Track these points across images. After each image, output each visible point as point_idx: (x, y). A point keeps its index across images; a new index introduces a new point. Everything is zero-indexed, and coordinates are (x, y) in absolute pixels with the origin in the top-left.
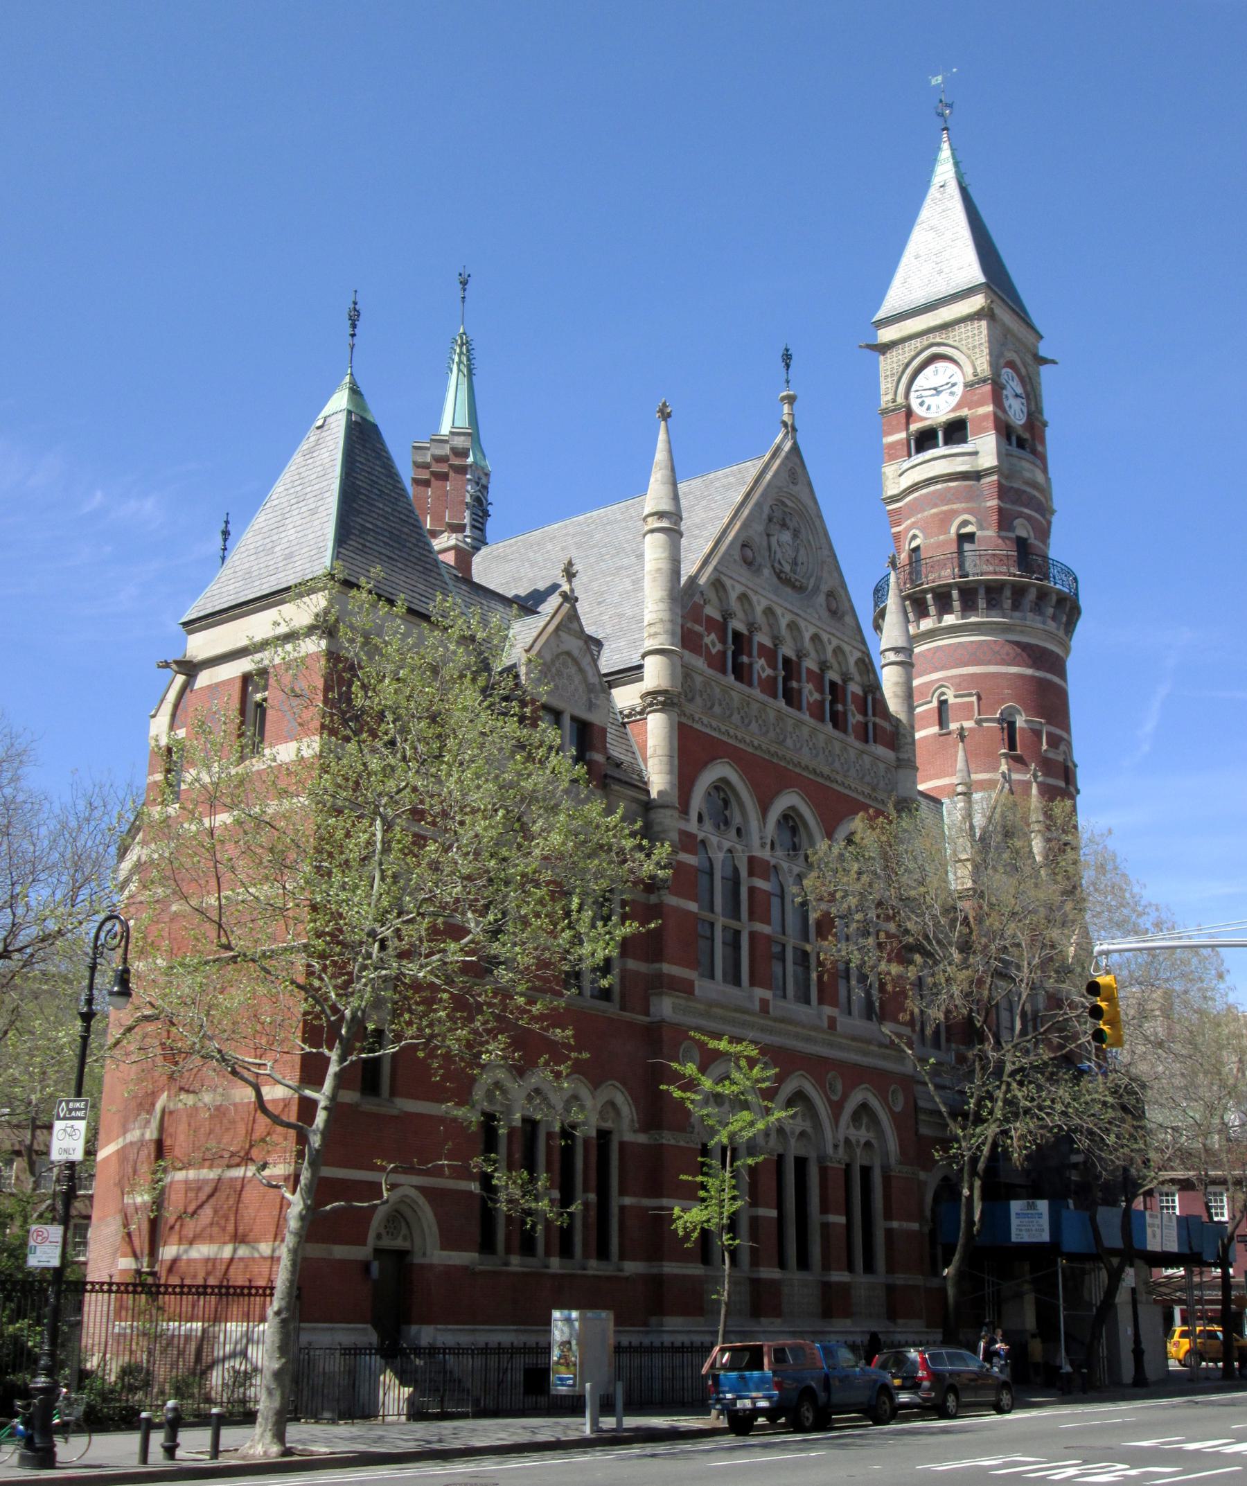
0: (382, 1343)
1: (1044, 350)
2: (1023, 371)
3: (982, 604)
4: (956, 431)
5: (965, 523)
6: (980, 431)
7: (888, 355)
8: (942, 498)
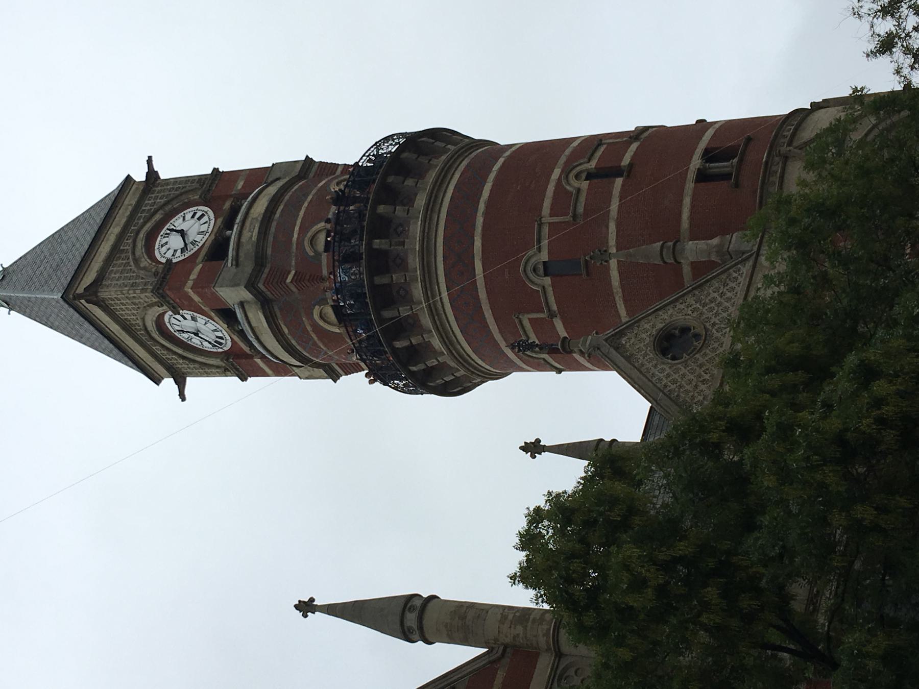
1: (140, 176)
2: (158, 217)
3: (404, 311)
4: (227, 315)
6: (218, 299)
8: (304, 338)
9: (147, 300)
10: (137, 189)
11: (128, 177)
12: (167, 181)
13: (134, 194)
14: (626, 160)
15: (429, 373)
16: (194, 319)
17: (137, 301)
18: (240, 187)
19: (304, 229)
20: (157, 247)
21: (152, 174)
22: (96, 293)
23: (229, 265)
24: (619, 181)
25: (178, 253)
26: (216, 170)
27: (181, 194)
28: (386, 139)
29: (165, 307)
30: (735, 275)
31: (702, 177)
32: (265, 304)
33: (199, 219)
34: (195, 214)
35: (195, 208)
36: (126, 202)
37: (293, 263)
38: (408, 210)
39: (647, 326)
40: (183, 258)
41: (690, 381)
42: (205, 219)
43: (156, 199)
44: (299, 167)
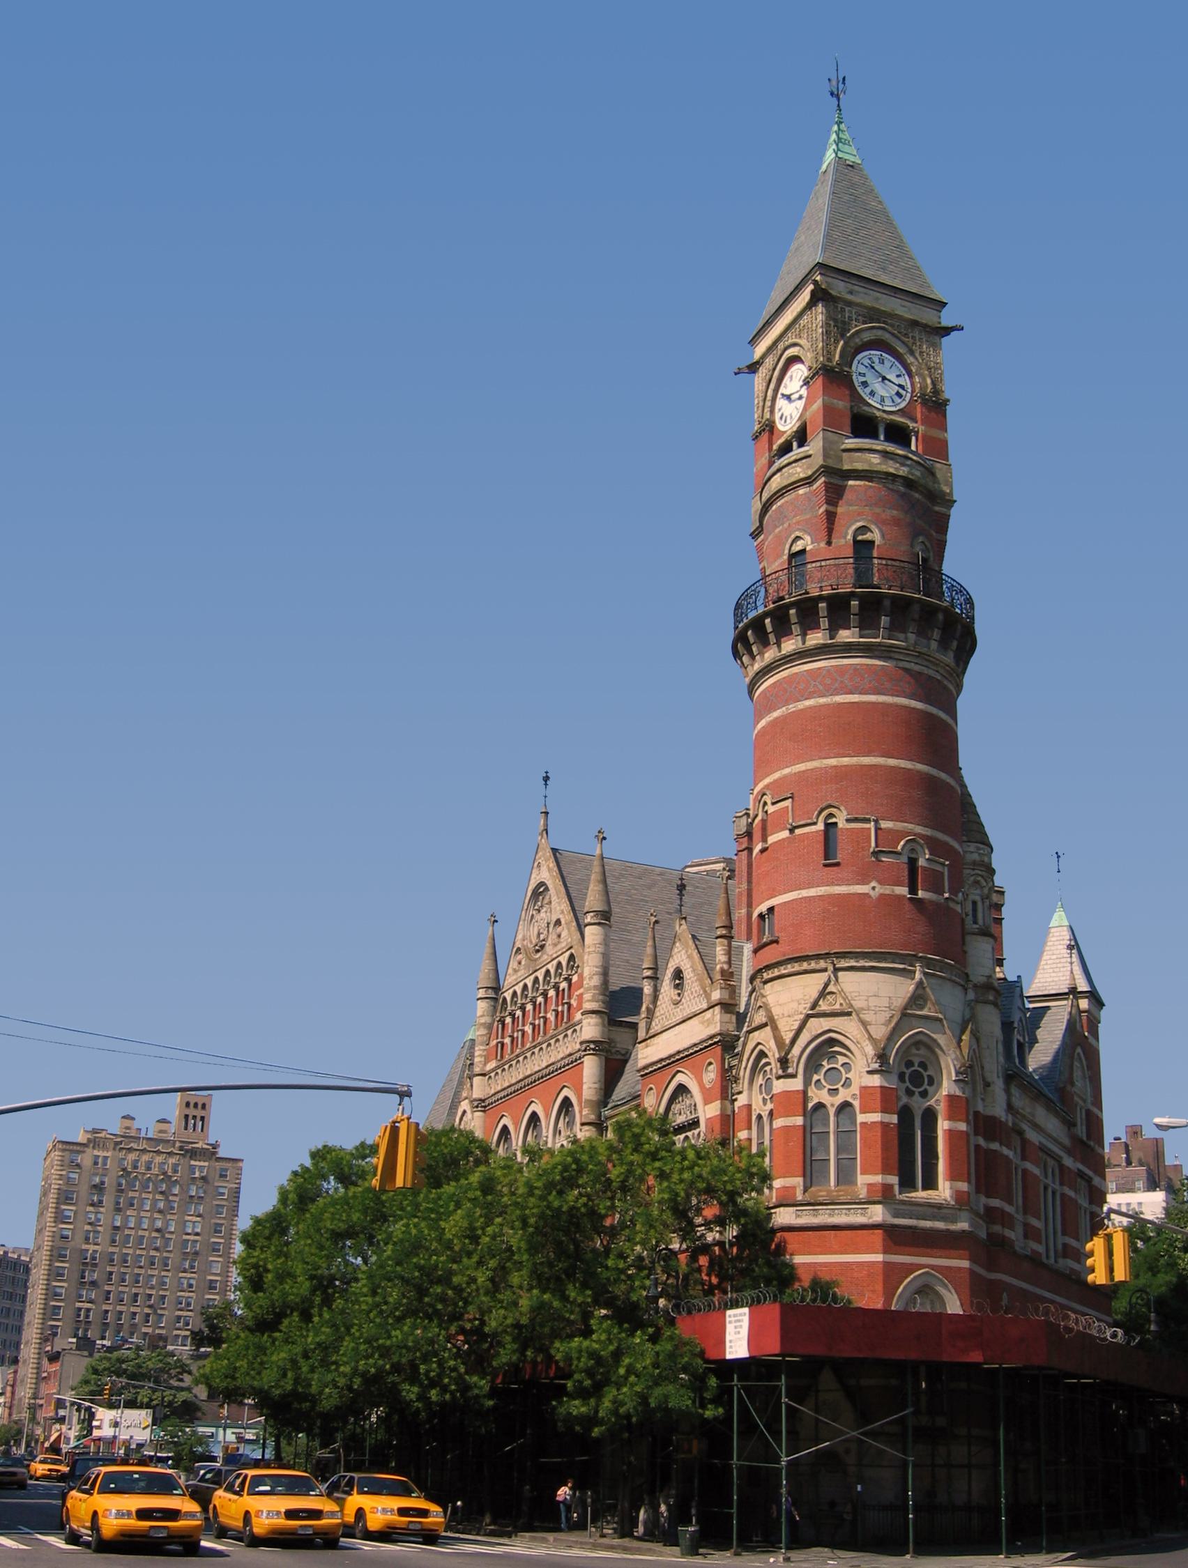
0: (574, 1494)
1: (946, 319)
16: (800, 398)
32: (808, 481)
33: (898, 394)
40: (856, 384)
42: (898, 400)
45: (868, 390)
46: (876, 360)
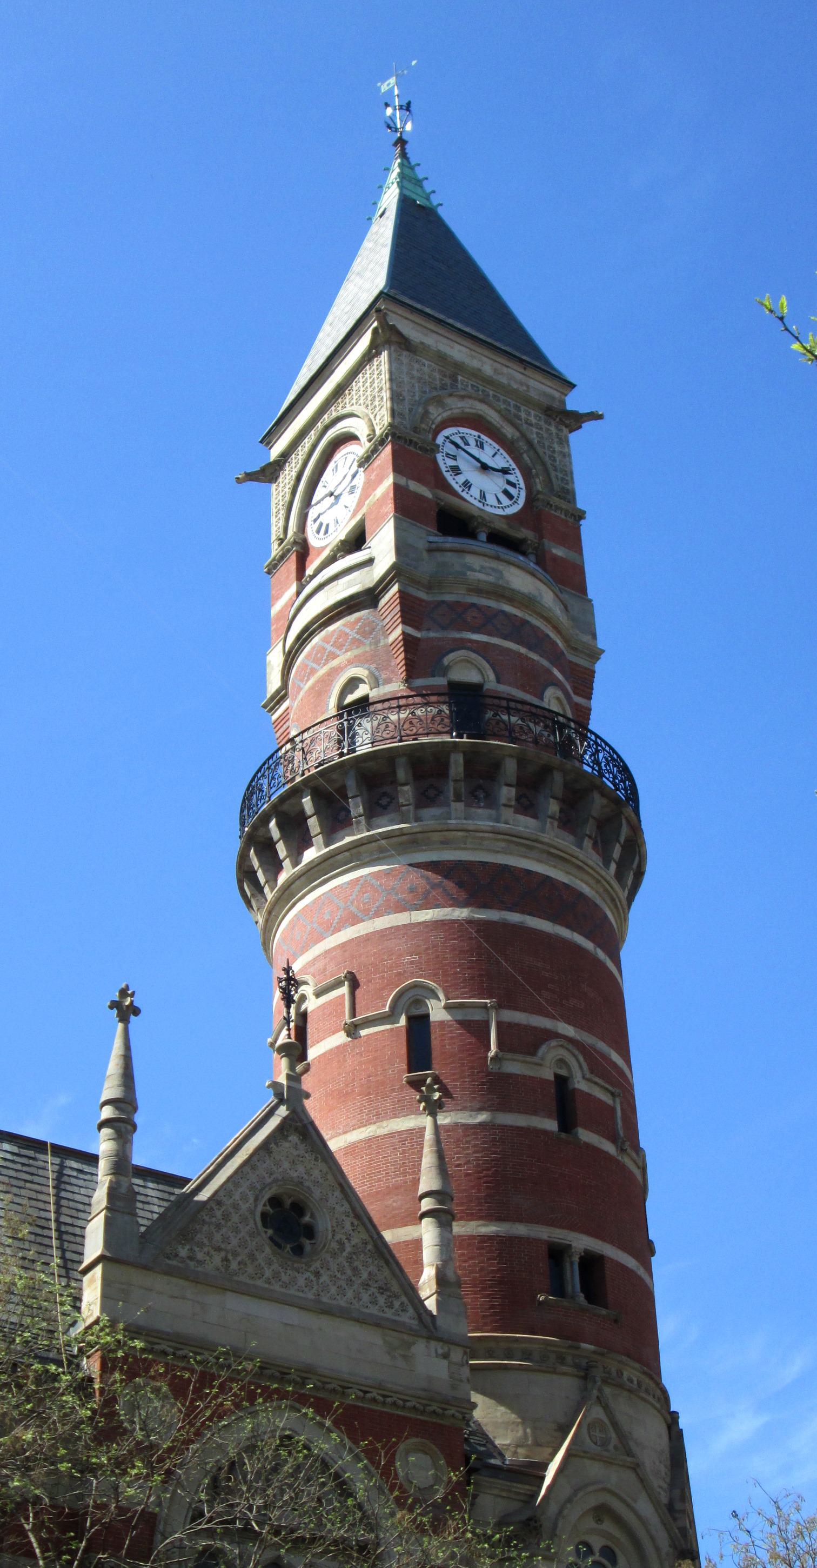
1: (574, 402)
2: (509, 431)
5: (353, 683)
6: (379, 521)
7: (280, 480)
9: (378, 417)
10: (554, 398)
11: (572, 386)
12: (564, 442)
13: (545, 394)
14: (585, 1135)
15: (267, 849)
17: (377, 403)
18: (554, 551)
19: (482, 649)
20: (462, 430)
21: (575, 420)
22: (388, 343)
23: (432, 539)
24: (551, 1125)
25: (451, 463)
26: (580, 515)
27: (544, 464)
28: (625, 770)
29: (368, 445)
30: (397, 1304)
31: (557, 1253)
33: (506, 492)
34: (513, 485)
35: (522, 485)
36: (532, 383)
37: (432, 634)
38: (510, 806)
39: (316, 1173)
40: (443, 469)
41: (226, 1239)
42: (505, 501)
43: (536, 427)
44: (586, 638)
45: (461, 479)
46: (472, 442)
